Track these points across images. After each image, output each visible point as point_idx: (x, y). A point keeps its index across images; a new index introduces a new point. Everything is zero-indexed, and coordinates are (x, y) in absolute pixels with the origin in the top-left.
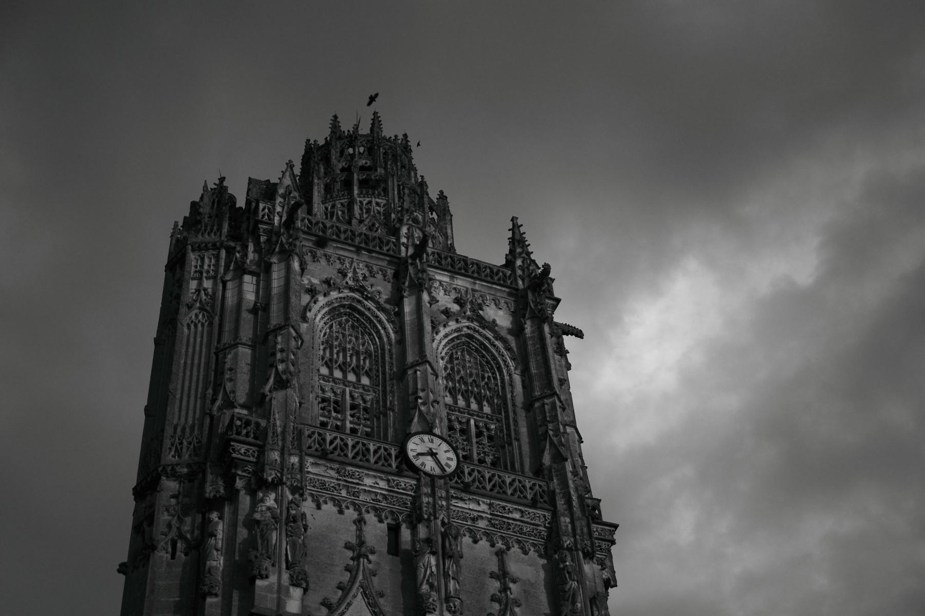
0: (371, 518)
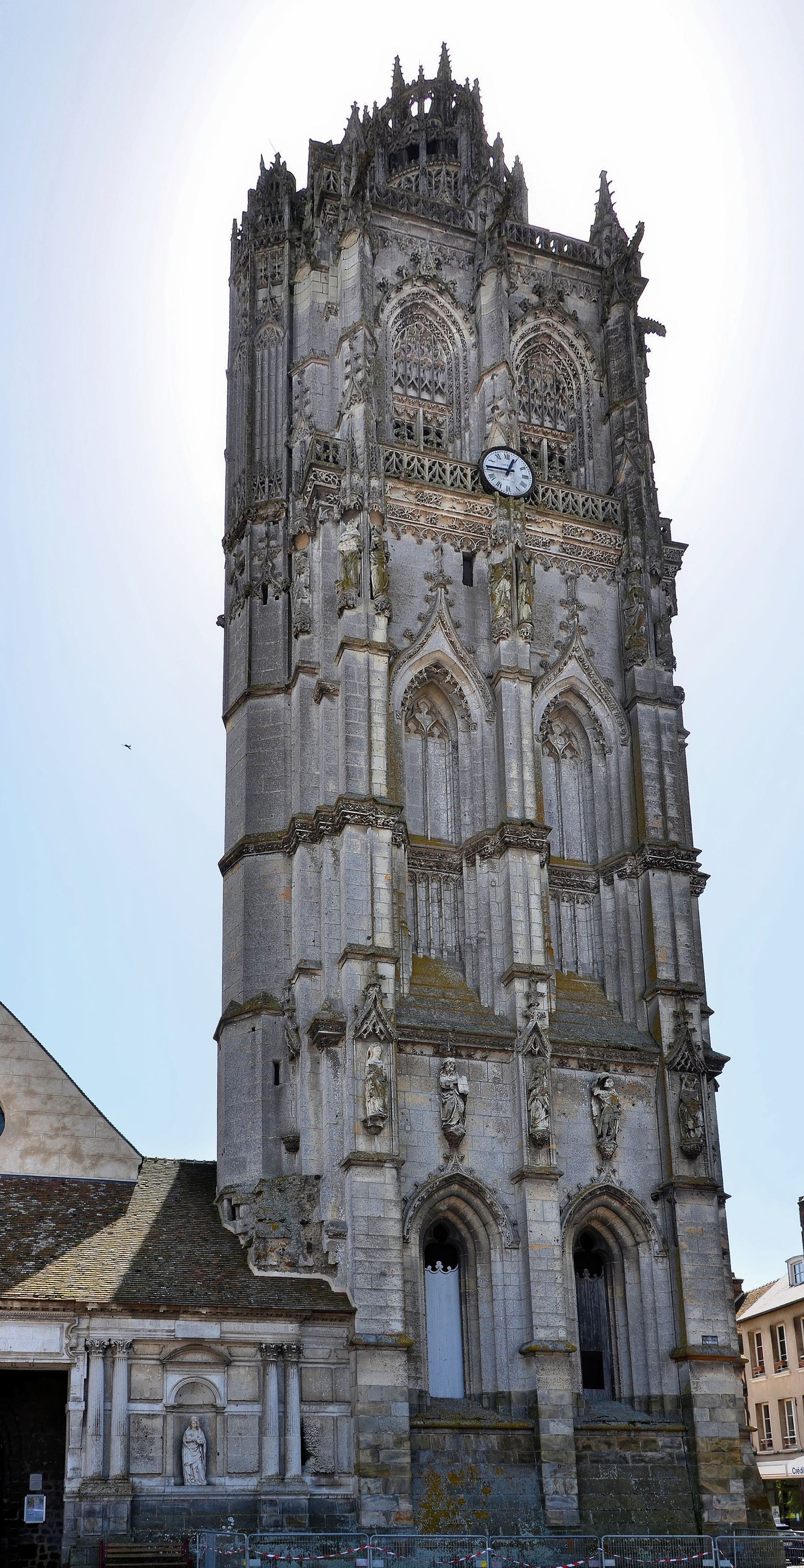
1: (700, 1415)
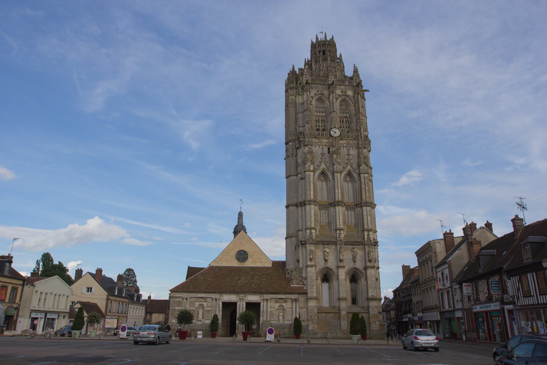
0: (325, 147)
1: (370, 310)
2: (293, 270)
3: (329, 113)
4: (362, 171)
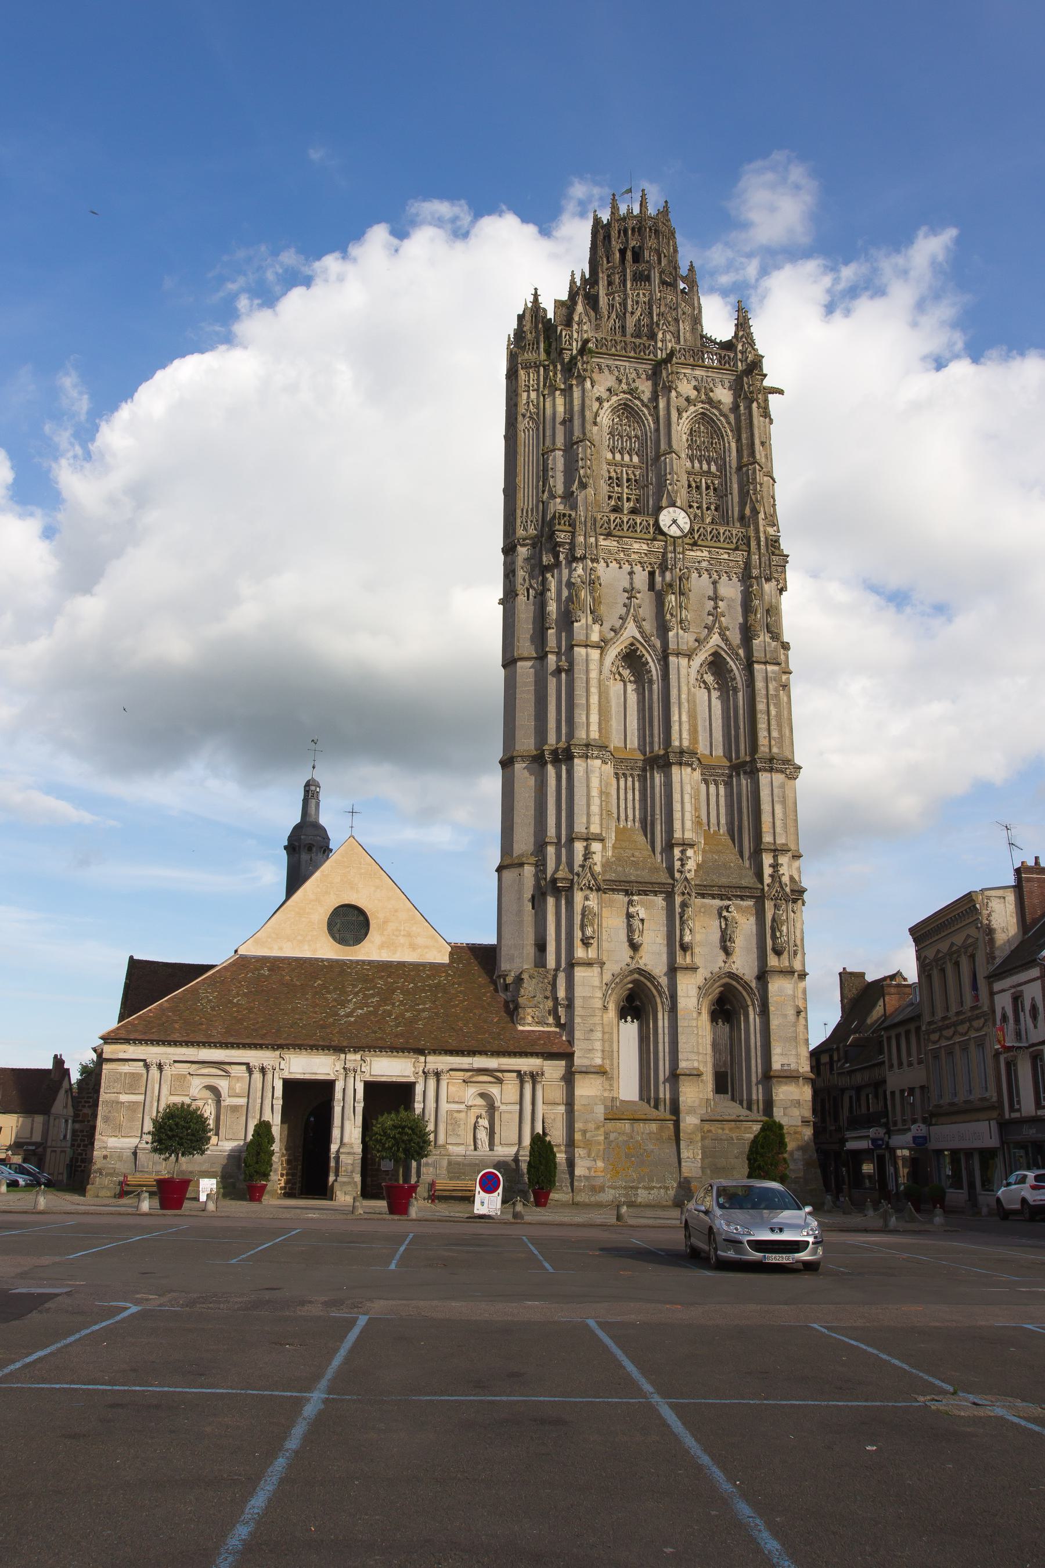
0: (638, 569)
2: (525, 976)
3: (655, 455)
4: (758, 654)
